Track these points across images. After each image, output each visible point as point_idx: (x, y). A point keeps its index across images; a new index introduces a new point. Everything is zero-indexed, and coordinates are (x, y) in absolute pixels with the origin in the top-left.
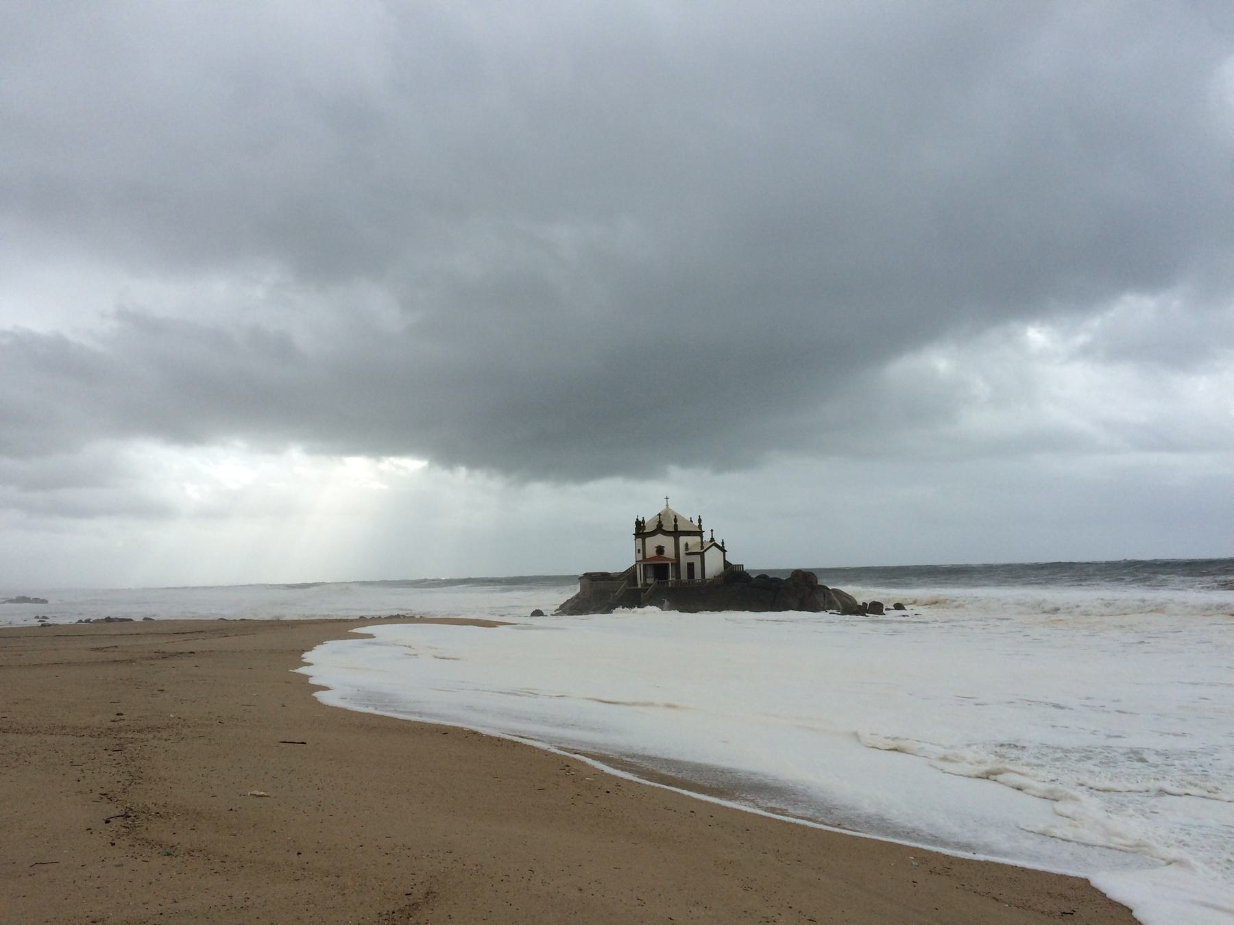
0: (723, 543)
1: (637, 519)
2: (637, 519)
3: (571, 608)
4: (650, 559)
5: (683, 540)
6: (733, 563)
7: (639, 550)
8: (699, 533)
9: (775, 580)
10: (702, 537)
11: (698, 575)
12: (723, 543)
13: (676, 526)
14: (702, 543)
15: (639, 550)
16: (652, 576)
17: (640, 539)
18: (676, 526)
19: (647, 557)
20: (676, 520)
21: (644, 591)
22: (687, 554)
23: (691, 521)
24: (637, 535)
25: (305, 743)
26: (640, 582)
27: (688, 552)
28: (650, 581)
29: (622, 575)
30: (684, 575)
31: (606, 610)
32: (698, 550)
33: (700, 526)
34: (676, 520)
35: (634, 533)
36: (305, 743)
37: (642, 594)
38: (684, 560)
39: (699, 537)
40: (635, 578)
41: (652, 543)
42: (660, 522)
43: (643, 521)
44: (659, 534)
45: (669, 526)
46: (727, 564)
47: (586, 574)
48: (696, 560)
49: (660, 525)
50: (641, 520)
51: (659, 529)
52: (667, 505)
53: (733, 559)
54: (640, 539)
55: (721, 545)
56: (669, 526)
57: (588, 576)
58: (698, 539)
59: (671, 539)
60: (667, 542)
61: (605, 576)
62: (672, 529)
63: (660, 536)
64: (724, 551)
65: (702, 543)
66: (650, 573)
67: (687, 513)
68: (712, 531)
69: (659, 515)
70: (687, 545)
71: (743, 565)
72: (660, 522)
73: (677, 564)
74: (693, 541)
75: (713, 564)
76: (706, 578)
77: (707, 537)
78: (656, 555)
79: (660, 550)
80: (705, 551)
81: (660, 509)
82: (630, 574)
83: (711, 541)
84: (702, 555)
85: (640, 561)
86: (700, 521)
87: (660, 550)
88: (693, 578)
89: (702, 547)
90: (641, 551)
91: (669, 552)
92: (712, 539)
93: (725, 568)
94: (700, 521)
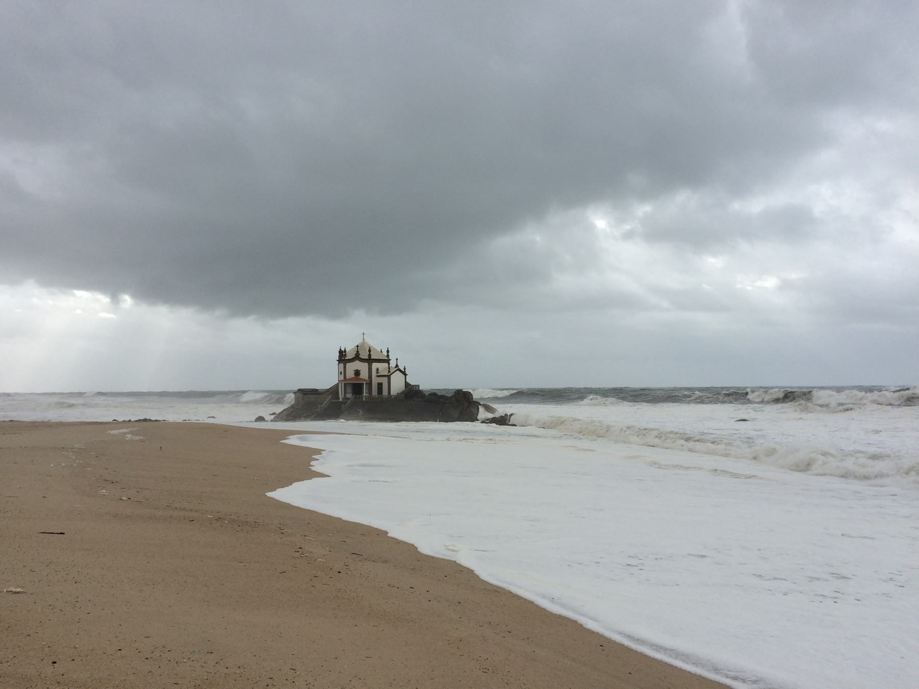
0: (405, 369)
1: (340, 349)
2: (340, 349)
3: (288, 415)
5: (375, 366)
6: (412, 383)
7: (341, 373)
8: (387, 361)
9: (442, 397)
10: (389, 364)
11: (385, 392)
12: (405, 369)
13: (370, 355)
14: (389, 368)
15: (341, 373)
16: (350, 391)
17: (342, 364)
18: (370, 355)
19: (347, 378)
20: (370, 351)
21: (344, 403)
22: (378, 376)
23: (381, 352)
24: (340, 361)
25: (64, 534)
26: (341, 396)
28: (349, 396)
29: (328, 390)
30: (375, 392)
31: (315, 417)
32: (386, 373)
33: (388, 356)
34: (370, 351)
35: (338, 359)
36: (64, 534)
37: (343, 405)
38: (375, 380)
39: (387, 364)
40: (338, 393)
41: (351, 367)
42: (358, 352)
43: (345, 351)
44: (357, 361)
45: (364, 355)
46: (407, 384)
47: (299, 390)
48: (384, 381)
49: (357, 355)
50: (343, 349)
51: (357, 357)
52: (364, 339)
53: (412, 381)
54: (342, 364)
55: (403, 370)
56: (364, 355)
57: (303, 393)
58: (386, 365)
59: (366, 365)
60: (363, 367)
61: (314, 392)
62: (367, 357)
64: (405, 375)
65: (389, 368)
66: (349, 390)
67: (378, 343)
68: (397, 359)
69: (357, 346)
70: (378, 369)
71: (419, 386)
72: (358, 352)
73: (370, 384)
74: (382, 367)
75: (397, 385)
76: (392, 394)
77: (393, 364)
78: (354, 376)
79: (357, 373)
80: (392, 374)
81: (358, 341)
82: (334, 391)
83: (396, 367)
84: (389, 377)
85: (342, 380)
86: (388, 351)
87: (357, 373)
88: (382, 394)
89: (389, 372)
90: (343, 373)
91: (364, 375)
92: (397, 366)
93: (406, 387)
94: (388, 351)
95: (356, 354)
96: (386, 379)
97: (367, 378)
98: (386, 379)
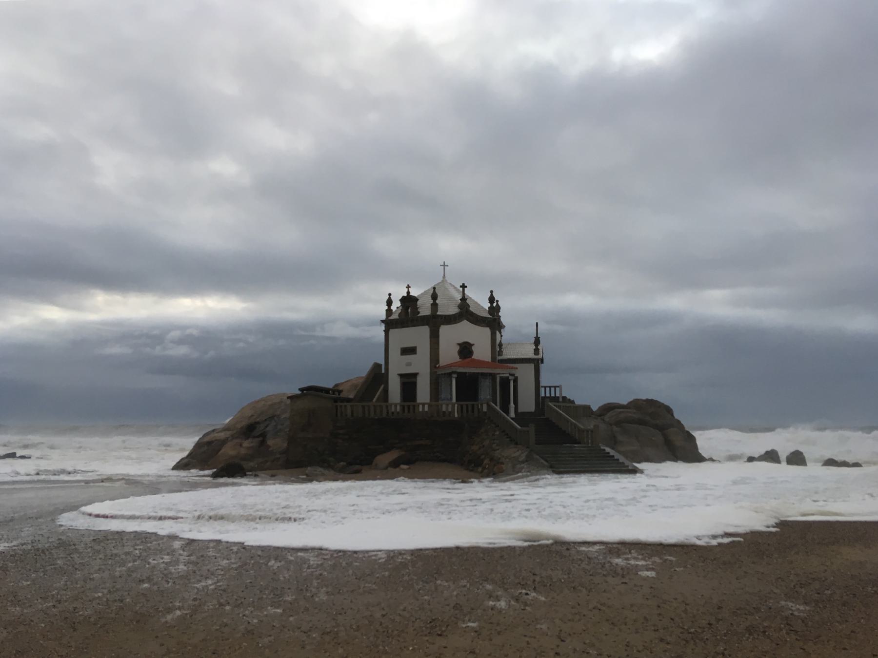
1: (408, 293)
2: (408, 293)
27: (500, 358)
35: (385, 319)
42: (464, 299)
44: (465, 322)
48: (525, 374)
59: (487, 331)
63: (465, 324)
64: (542, 362)
68: (537, 323)
72: (464, 299)
79: (466, 350)
84: (537, 363)
86: (498, 308)
87: (466, 350)
91: (482, 352)
95: (460, 307)
96: (532, 366)
97: (489, 359)
98: (532, 366)
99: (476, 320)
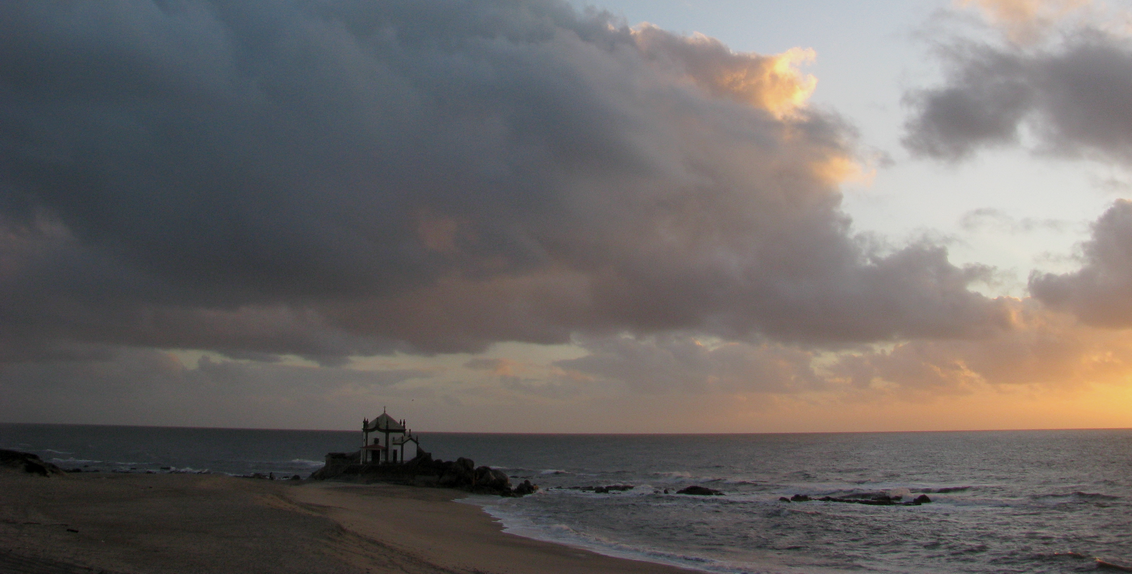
4: (371, 446)
5: (391, 435)
11: (399, 459)
13: (387, 426)
18: (387, 426)
30: (391, 459)
38: (392, 448)
41: (373, 435)
45: (383, 426)
56: (383, 426)
58: (402, 434)
59: (384, 434)
73: (386, 450)
74: (398, 436)
75: (410, 452)
79: (377, 441)
84: (402, 445)
87: (377, 441)
91: (382, 443)
99: (381, 430)
